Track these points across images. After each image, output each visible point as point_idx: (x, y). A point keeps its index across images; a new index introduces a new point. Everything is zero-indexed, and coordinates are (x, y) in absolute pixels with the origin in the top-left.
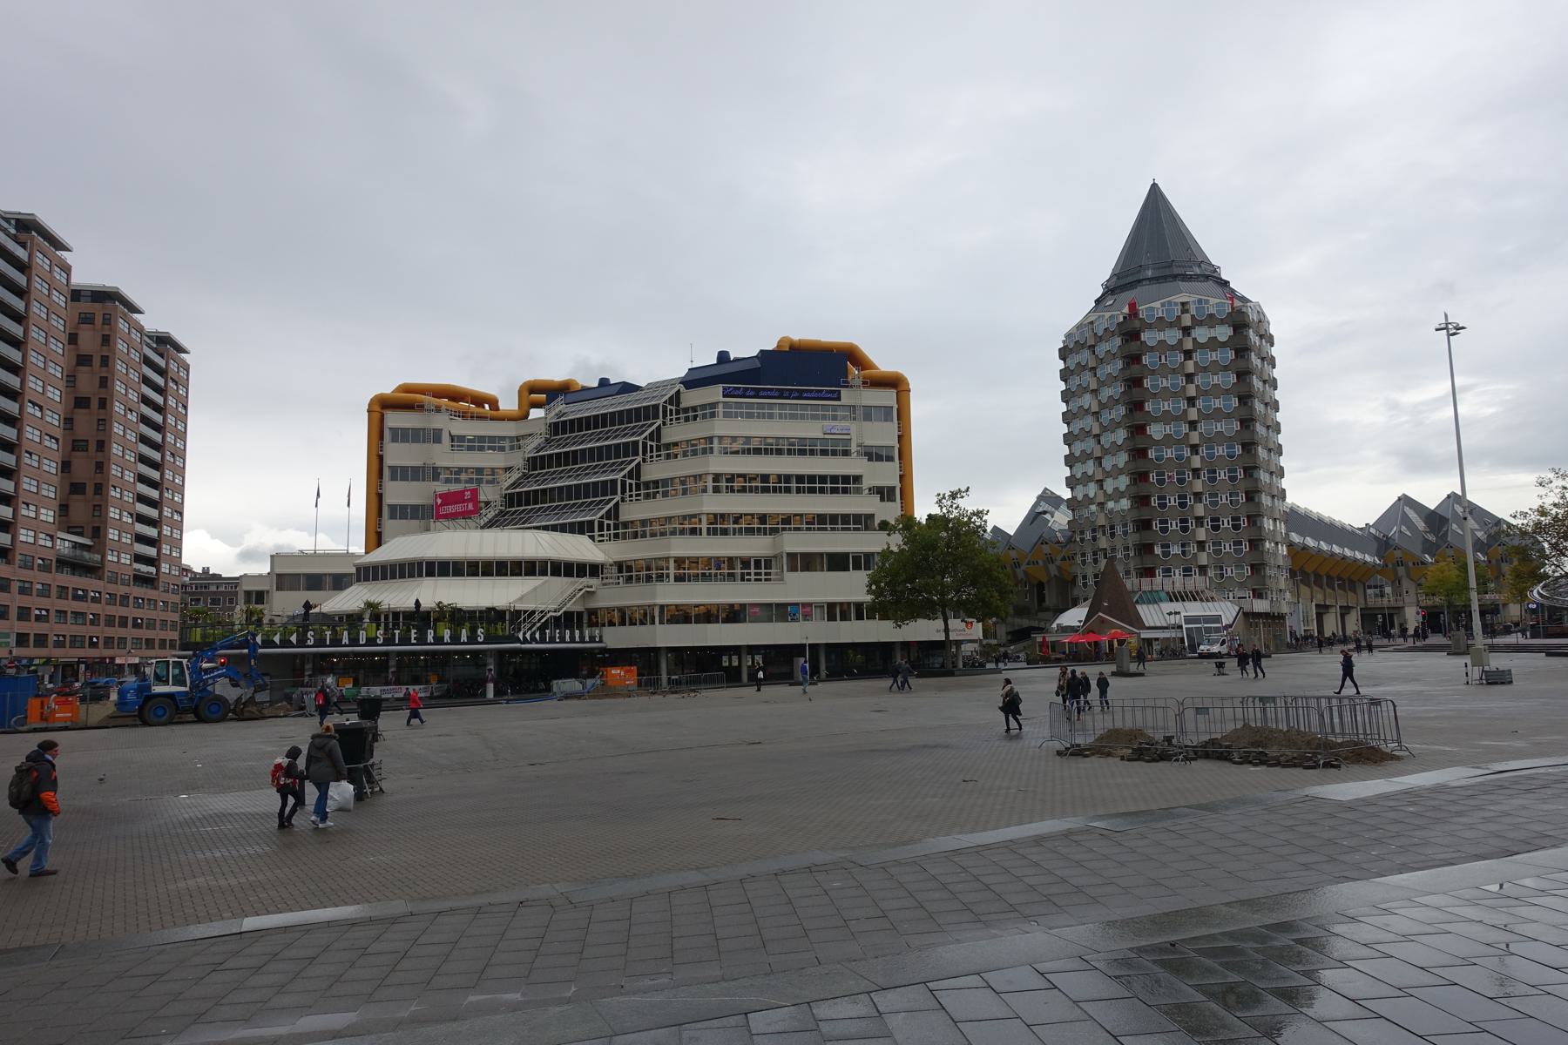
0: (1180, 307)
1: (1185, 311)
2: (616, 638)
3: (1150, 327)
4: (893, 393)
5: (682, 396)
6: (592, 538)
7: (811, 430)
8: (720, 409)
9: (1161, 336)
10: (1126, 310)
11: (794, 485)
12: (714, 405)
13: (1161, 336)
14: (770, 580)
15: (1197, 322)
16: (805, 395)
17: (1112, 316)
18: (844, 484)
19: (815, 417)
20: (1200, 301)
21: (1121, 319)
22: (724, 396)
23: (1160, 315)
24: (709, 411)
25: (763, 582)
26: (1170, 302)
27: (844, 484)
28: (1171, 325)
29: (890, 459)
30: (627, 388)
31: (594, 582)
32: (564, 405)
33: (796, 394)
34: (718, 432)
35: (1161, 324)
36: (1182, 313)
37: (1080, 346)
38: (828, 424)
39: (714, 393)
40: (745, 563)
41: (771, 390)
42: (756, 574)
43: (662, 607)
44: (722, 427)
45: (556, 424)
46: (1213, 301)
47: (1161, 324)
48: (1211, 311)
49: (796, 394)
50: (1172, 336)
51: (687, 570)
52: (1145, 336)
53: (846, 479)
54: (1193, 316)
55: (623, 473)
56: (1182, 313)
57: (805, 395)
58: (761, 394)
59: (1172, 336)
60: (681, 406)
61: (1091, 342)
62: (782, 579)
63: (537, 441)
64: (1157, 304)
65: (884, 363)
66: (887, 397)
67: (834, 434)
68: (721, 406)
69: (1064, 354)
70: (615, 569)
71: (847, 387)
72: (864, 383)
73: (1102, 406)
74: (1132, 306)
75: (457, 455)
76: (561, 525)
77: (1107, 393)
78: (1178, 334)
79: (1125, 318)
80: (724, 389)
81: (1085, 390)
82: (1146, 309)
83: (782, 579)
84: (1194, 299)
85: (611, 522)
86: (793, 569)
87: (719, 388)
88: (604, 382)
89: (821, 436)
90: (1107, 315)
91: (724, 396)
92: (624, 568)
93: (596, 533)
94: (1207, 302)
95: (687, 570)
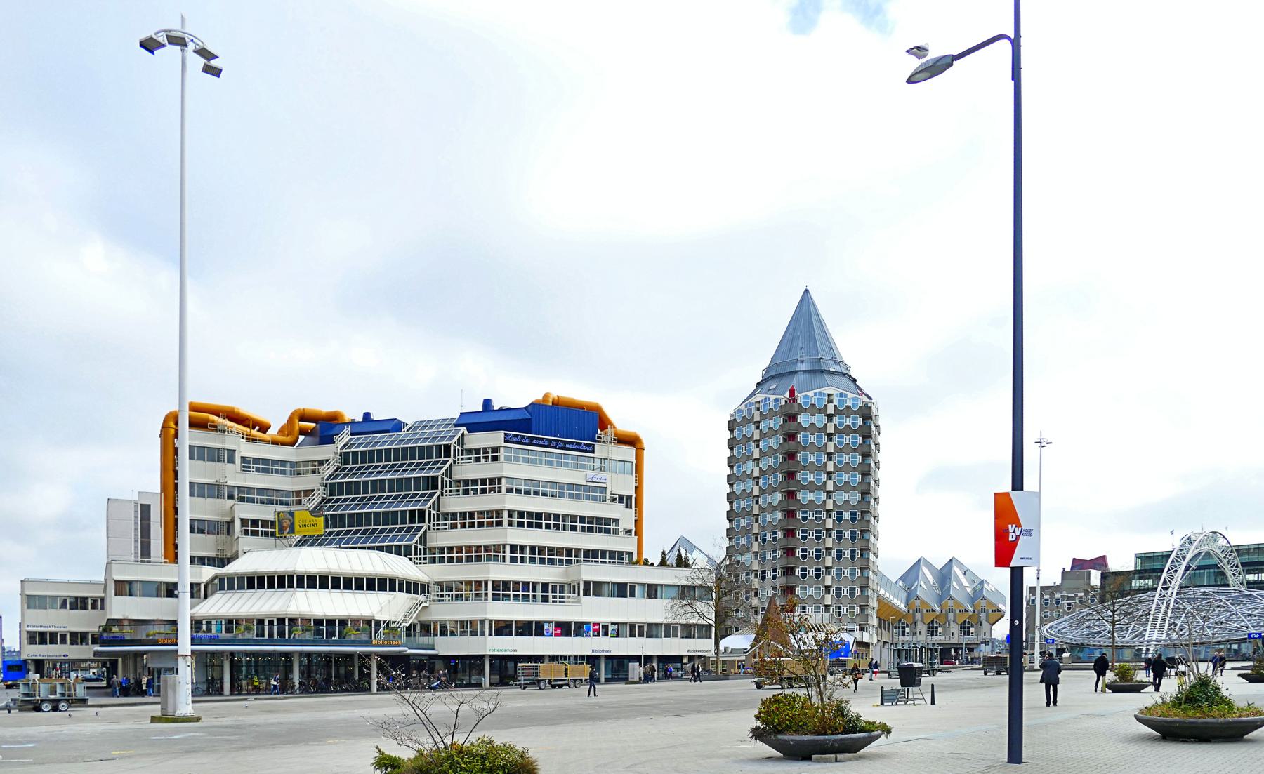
0: (826, 398)
1: (830, 402)
2: (447, 646)
3: (805, 411)
4: (632, 450)
5: (465, 437)
6: (410, 559)
7: (576, 477)
8: (502, 454)
9: (812, 420)
10: (787, 395)
12: (495, 450)
13: (812, 420)
14: (563, 602)
16: (568, 446)
17: (776, 400)
18: (605, 525)
19: (584, 467)
20: (841, 395)
21: (784, 403)
22: (505, 442)
23: (813, 403)
24: (493, 454)
25: (558, 604)
26: (820, 393)
28: (820, 411)
30: (396, 426)
31: (422, 598)
32: (350, 437)
33: (561, 445)
34: (505, 474)
35: (813, 410)
36: (828, 403)
37: (747, 421)
38: (590, 474)
39: (495, 438)
40: (545, 586)
41: (542, 439)
42: (560, 597)
43: (490, 621)
44: (508, 469)
45: (347, 454)
46: (851, 395)
47: (813, 410)
48: (849, 404)
49: (561, 445)
50: (819, 420)
51: (504, 590)
52: (800, 419)
53: (607, 521)
54: (835, 406)
55: (428, 505)
56: (828, 403)
57: (568, 446)
58: (535, 442)
59: (819, 420)
60: (465, 447)
61: (757, 418)
62: (579, 602)
63: (327, 471)
64: (811, 393)
66: (628, 453)
67: (593, 482)
68: (502, 450)
70: (437, 588)
71: (600, 442)
72: (615, 440)
74: (792, 392)
75: (248, 475)
76: (386, 546)
78: (825, 420)
79: (786, 401)
80: (506, 435)
82: (803, 396)
83: (579, 602)
84: (837, 392)
85: (422, 547)
86: (586, 593)
87: (502, 433)
89: (585, 483)
90: (773, 397)
91: (505, 442)
92: (445, 587)
93: (413, 556)
94: (846, 396)
95: (504, 590)
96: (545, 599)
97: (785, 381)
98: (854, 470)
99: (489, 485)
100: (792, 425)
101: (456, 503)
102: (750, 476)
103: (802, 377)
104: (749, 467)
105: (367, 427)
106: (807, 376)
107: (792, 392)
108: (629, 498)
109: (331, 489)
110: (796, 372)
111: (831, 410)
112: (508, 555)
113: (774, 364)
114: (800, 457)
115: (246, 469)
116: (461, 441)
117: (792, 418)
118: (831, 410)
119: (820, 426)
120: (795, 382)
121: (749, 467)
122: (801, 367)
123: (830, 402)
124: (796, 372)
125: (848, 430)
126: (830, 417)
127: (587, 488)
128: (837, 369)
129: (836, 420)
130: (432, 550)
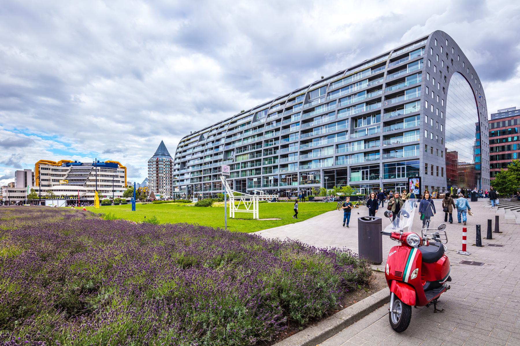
2: (89, 199)
4: (124, 169)
7: (114, 174)
8: (100, 171)
9: (161, 163)
15: (165, 162)
18: (118, 181)
27: (118, 181)
29: (124, 177)
30: (81, 164)
39: (99, 168)
47: (161, 161)
52: (159, 163)
65: (123, 164)
66: (123, 170)
69: (149, 162)
74: (158, 158)
77: (154, 169)
88: (76, 162)
96: (106, 193)
103: (160, 156)
104: (151, 169)
105: (76, 164)
108: (124, 177)
111: (164, 161)
112: (100, 186)
113: (156, 153)
115: (52, 171)
118: (164, 161)
121: (151, 169)
128: (167, 154)
130: (87, 185)
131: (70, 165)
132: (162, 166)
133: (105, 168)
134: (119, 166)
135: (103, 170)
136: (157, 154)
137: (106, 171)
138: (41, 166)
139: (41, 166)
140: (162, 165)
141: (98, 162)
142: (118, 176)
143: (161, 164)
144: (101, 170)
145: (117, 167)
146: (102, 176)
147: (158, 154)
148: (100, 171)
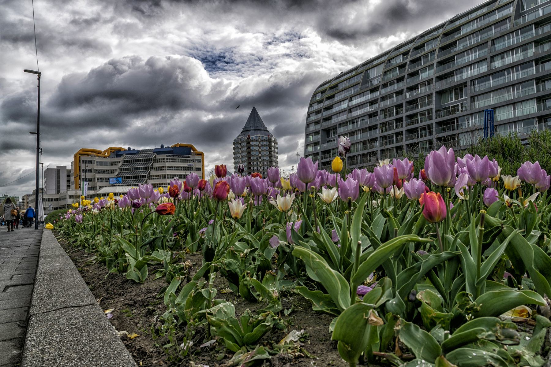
1: (260, 138)
3: (252, 141)
8: (166, 160)
10: (247, 137)
11: (183, 177)
12: (164, 159)
28: (257, 141)
29: (200, 170)
35: (255, 141)
39: (165, 156)
45: (125, 161)
46: (265, 136)
47: (255, 141)
50: (257, 143)
52: (251, 143)
63: (120, 165)
64: (254, 136)
73: (242, 157)
74: (249, 136)
75: (99, 167)
77: (243, 154)
78: (258, 143)
81: (239, 153)
87: (166, 155)
97: (247, 132)
98: (267, 156)
99: (162, 168)
100: (249, 145)
101: (154, 173)
102: (239, 157)
103: (252, 131)
104: (239, 155)
106: (253, 131)
107: (249, 136)
108: (200, 168)
109: (121, 170)
110: (250, 130)
111: (259, 140)
113: (245, 128)
114: (251, 153)
115: (97, 165)
116: (155, 157)
117: (249, 143)
118: (259, 140)
119: (257, 144)
120: (250, 133)
121: (239, 155)
122: (252, 128)
123: (260, 138)
124: (250, 130)
125: (265, 145)
126: (259, 142)
127: (188, 168)
128: (262, 129)
129: (261, 143)
131: (122, 155)
132: (257, 148)
133: (173, 156)
134: (192, 151)
135: (170, 159)
136: (246, 129)
137: (174, 160)
138: (83, 158)
139: (83, 158)
140: (257, 146)
141: (162, 146)
142: (192, 168)
143: (255, 145)
144: (167, 159)
145: (190, 154)
146: (170, 168)
147: (249, 129)
148: (166, 160)
